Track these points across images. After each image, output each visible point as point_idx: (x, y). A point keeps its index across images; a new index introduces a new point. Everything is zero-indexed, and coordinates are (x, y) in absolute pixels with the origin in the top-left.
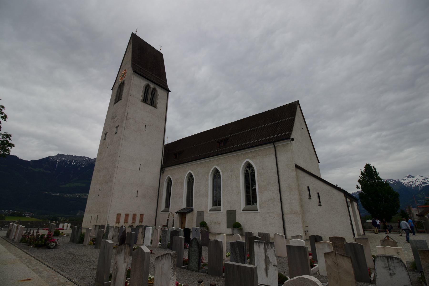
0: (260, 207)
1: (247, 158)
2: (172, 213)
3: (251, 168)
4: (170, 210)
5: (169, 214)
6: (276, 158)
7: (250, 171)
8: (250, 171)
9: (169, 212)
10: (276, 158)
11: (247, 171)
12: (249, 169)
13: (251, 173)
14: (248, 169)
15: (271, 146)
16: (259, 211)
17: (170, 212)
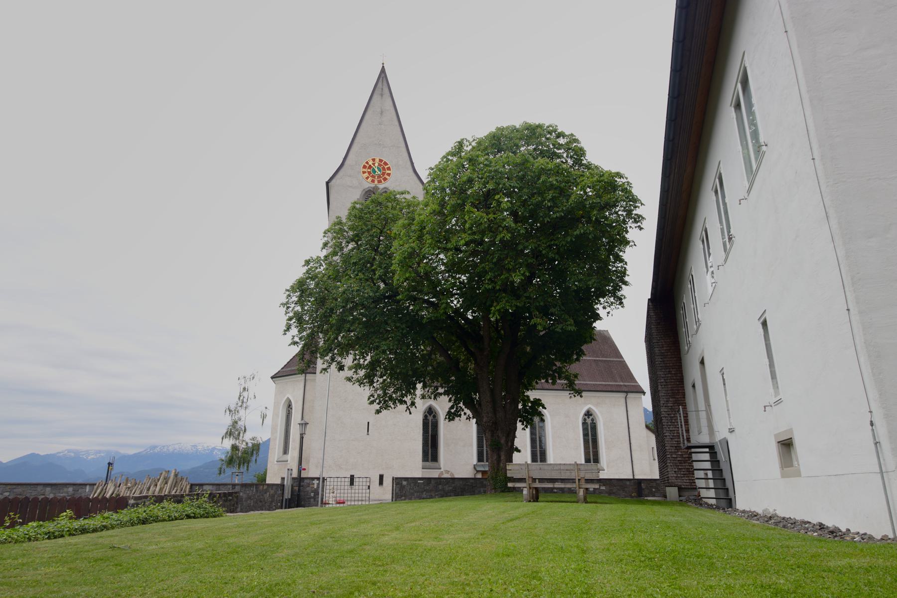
0: (608, 466)
1: (589, 404)
2: (449, 471)
3: (591, 417)
4: (442, 466)
5: (439, 473)
6: (627, 411)
7: (589, 421)
8: (589, 421)
9: (440, 469)
10: (627, 411)
11: (585, 420)
12: (589, 418)
13: (591, 423)
14: (586, 417)
15: (623, 395)
16: (606, 471)
17: (442, 470)
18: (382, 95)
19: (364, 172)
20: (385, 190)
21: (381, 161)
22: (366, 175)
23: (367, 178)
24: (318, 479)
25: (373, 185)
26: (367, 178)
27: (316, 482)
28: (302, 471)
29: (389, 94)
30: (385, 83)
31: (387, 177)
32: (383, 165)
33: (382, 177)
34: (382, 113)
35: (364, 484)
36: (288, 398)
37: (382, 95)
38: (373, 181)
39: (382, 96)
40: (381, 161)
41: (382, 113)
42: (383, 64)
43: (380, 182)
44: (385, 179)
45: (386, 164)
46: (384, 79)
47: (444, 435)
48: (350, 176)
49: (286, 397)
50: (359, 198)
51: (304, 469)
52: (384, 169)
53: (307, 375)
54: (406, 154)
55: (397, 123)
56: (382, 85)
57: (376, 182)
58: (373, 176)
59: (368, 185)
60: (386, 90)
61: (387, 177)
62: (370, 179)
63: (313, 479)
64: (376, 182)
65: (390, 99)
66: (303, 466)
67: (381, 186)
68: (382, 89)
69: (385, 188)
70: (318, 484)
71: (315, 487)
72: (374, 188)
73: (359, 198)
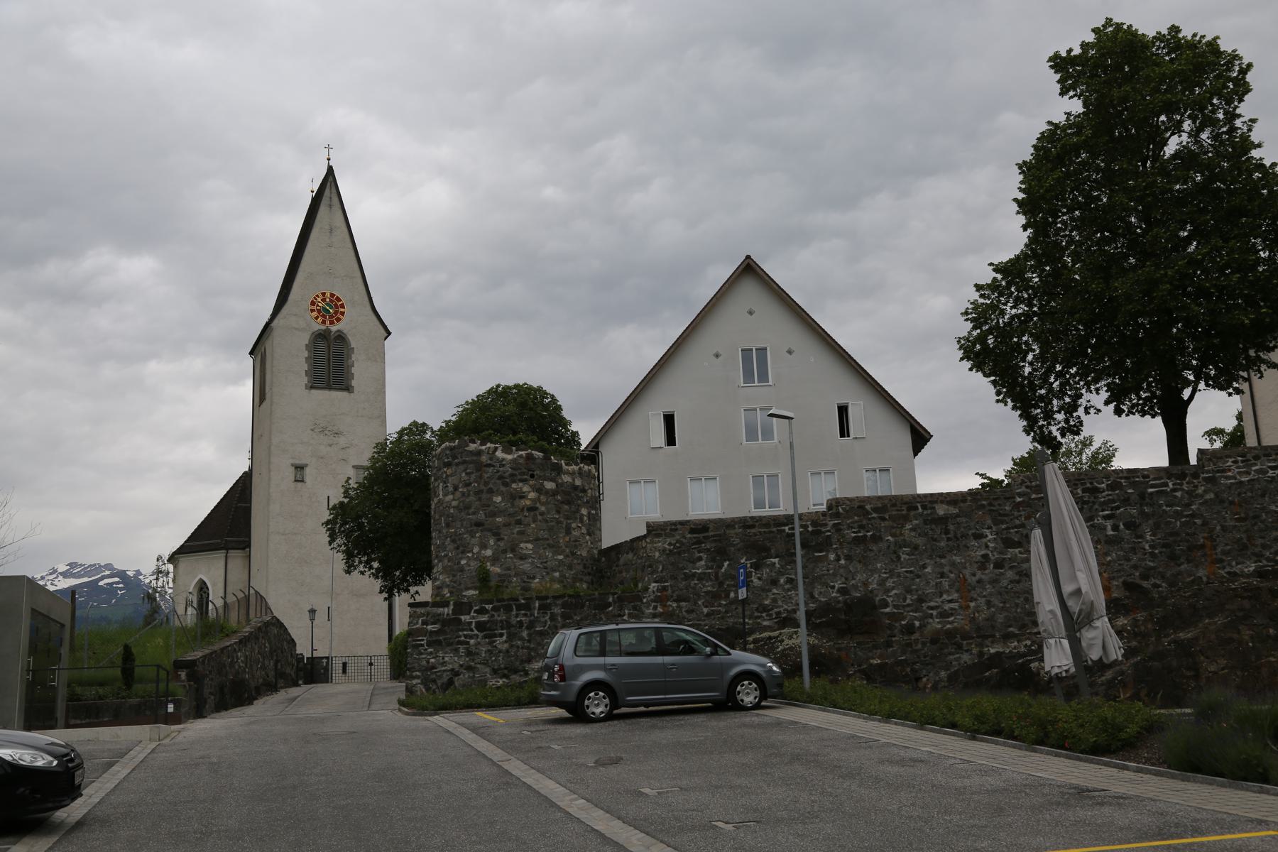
18: (330, 206)
19: (312, 311)
20: (338, 333)
21: (332, 295)
22: (315, 314)
23: (317, 318)
24: (327, 658)
25: (323, 327)
26: (317, 318)
27: (325, 661)
28: (314, 652)
29: (339, 206)
30: (334, 190)
31: (341, 317)
32: (335, 301)
33: (334, 317)
34: (331, 231)
35: (366, 661)
36: (201, 579)
37: (330, 206)
38: (324, 322)
39: (331, 208)
40: (332, 295)
41: (331, 231)
42: (329, 159)
43: (332, 323)
44: (339, 320)
45: (338, 299)
46: (333, 184)
47: (400, 620)
48: (295, 315)
49: (197, 580)
50: (307, 343)
51: (316, 650)
52: (336, 306)
53: (230, 551)
54: (362, 287)
55: (350, 245)
56: (331, 193)
57: (328, 323)
58: (324, 316)
59: (318, 326)
60: (335, 199)
61: (341, 317)
62: (320, 320)
63: (322, 658)
64: (328, 323)
65: (340, 213)
66: (314, 648)
67: (334, 328)
68: (331, 198)
69: (338, 331)
70: (327, 663)
71: (325, 664)
72: (325, 331)
73: (307, 343)
